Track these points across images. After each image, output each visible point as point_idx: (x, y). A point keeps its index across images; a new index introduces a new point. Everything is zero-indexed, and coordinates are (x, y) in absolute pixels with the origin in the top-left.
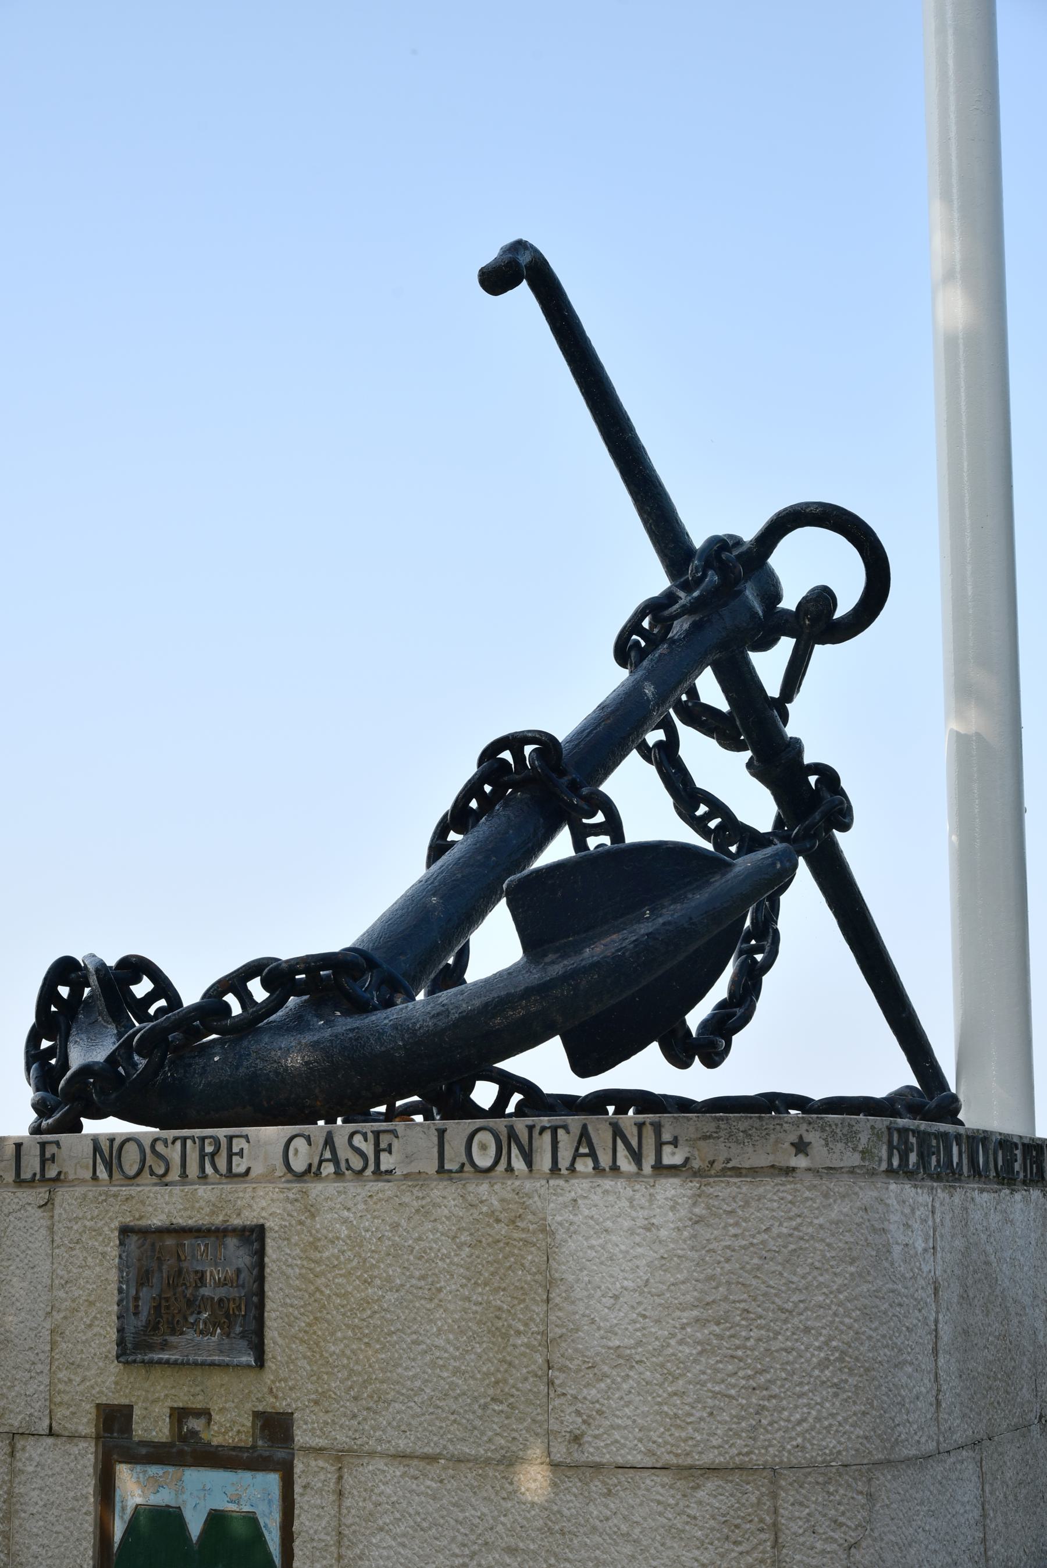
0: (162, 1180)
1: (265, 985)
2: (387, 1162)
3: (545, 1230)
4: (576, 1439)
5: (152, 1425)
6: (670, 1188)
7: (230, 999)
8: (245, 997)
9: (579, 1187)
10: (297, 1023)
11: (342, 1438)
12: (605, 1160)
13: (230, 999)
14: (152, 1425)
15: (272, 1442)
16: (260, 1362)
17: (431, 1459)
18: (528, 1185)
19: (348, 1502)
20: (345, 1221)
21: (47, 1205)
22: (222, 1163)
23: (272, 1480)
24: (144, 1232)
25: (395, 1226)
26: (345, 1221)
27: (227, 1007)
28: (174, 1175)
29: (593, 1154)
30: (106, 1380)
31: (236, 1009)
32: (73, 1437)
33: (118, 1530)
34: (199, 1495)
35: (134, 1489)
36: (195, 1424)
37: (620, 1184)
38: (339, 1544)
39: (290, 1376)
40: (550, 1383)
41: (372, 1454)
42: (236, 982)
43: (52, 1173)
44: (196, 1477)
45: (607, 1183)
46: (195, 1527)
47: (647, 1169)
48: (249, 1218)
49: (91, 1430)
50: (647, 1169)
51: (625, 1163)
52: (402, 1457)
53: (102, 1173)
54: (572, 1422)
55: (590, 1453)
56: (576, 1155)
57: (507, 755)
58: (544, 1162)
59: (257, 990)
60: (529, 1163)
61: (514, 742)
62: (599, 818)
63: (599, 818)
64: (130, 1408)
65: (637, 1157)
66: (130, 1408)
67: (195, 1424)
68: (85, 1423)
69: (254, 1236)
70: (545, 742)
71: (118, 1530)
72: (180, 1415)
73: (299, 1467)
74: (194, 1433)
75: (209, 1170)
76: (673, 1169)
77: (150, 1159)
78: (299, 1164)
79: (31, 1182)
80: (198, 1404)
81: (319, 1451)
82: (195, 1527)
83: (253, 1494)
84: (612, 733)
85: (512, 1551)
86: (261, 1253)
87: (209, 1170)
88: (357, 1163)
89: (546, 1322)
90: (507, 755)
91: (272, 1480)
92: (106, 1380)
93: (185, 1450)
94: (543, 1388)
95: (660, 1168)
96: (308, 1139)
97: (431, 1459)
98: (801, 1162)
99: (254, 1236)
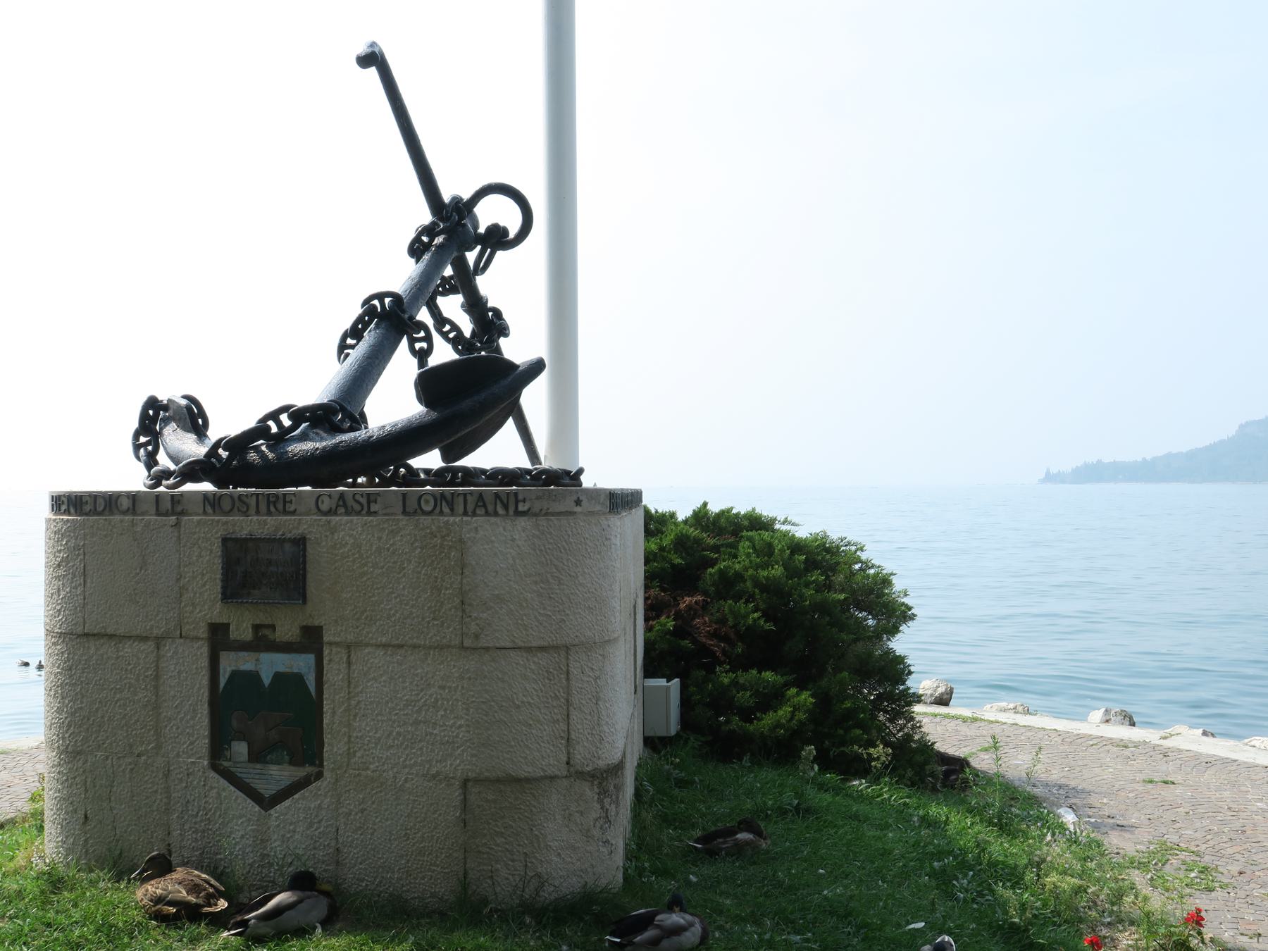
0: (246, 514)
1: (290, 417)
2: (374, 507)
3: (461, 541)
4: (477, 636)
5: (241, 629)
6: (522, 522)
7: (271, 423)
8: (279, 424)
9: (479, 520)
10: (303, 437)
11: (350, 637)
12: (490, 508)
13: (271, 423)
14: (241, 629)
15: (311, 640)
16: (305, 602)
17: (401, 646)
18: (452, 519)
19: (353, 667)
20: (351, 536)
21: (177, 525)
22: (280, 506)
23: (310, 658)
24: (236, 540)
25: (380, 539)
26: (351, 536)
27: (269, 428)
28: (252, 510)
29: (485, 506)
30: (216, 612)
31: (274, 429)
32: (198, 639)
33: (223, 682)
34: (269, 665)
35: (230, 663)
36: (267, 632)
37: (498, 520)
38: (349, 687)
39: (322, 608)
40: (463, 611)
41: (367, 645)
42: (274, 415)
43: (179, 509)
44: (266, 657)
45: (493, 519)
46: (267, 681)
47: (511, 511)
48: (296, 533)
49: (205, 635)
50: (511, 511)
51: (501, 511)
52: (385, 646)
53: (209, 510)
54: (473, 628)
55: (483, 643)
56: (477, 506)
57: (376, 302)
58: (461, 509)
59: (285, 420)
60: (452, 510)
61: (380, 296)
62: (422, 334)
63: (422, 334)
64: (228, 624)
65: (506, 507)
66: (228, 624)
67: (267, 632)
68: (203, 632)
69: (301, 542)
70: (396, 297)
71: (223, 682)
72: (257, 628)
73: (326, 651)
74: (265, 636)
75: (272, 509)
76: (524, 514)
77: (237, 503)
78: (324, 507)
79: (166, 514)
80: (268, 621)
81: (337, 644)
82: (267, 681)
83: (301, 663)
84: (426, 290)
85: (443, 688)
86: (305, 550)
87: (272, 509)
88: (357, 507)
89: (461, 583)
90: (376, 302)
91: (310, 658)
92: (216, 612)
93: (262, 642)
94: (460, 614)
95: (518, 513)
96: (330, 496)
97: (401, 646)
98: (578, 509)
99: (301, 542)
